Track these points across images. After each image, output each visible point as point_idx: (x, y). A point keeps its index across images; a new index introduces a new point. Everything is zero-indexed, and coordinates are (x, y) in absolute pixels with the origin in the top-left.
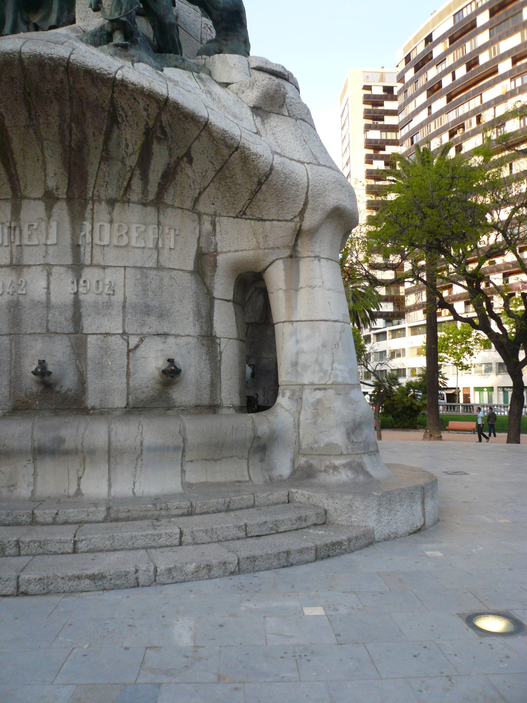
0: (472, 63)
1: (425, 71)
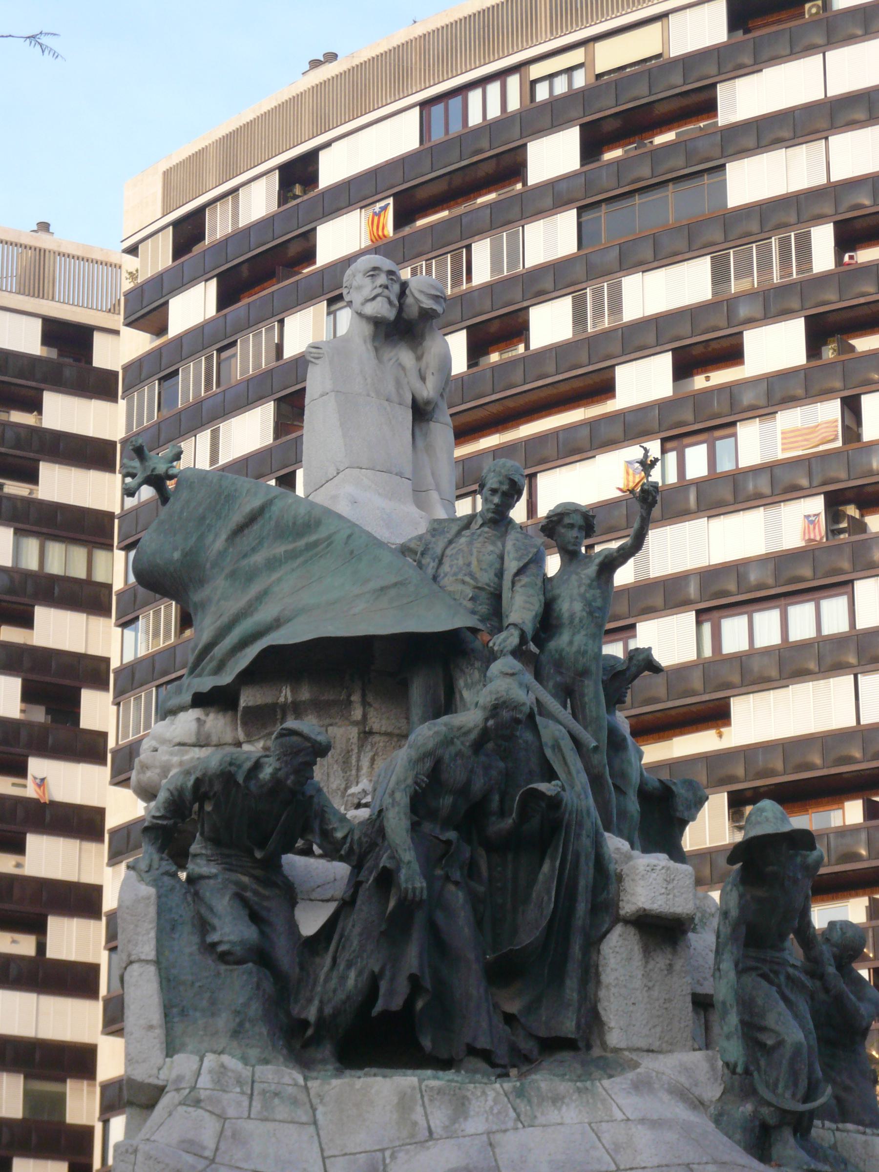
0: (495, 329)
1: (277, 313)
